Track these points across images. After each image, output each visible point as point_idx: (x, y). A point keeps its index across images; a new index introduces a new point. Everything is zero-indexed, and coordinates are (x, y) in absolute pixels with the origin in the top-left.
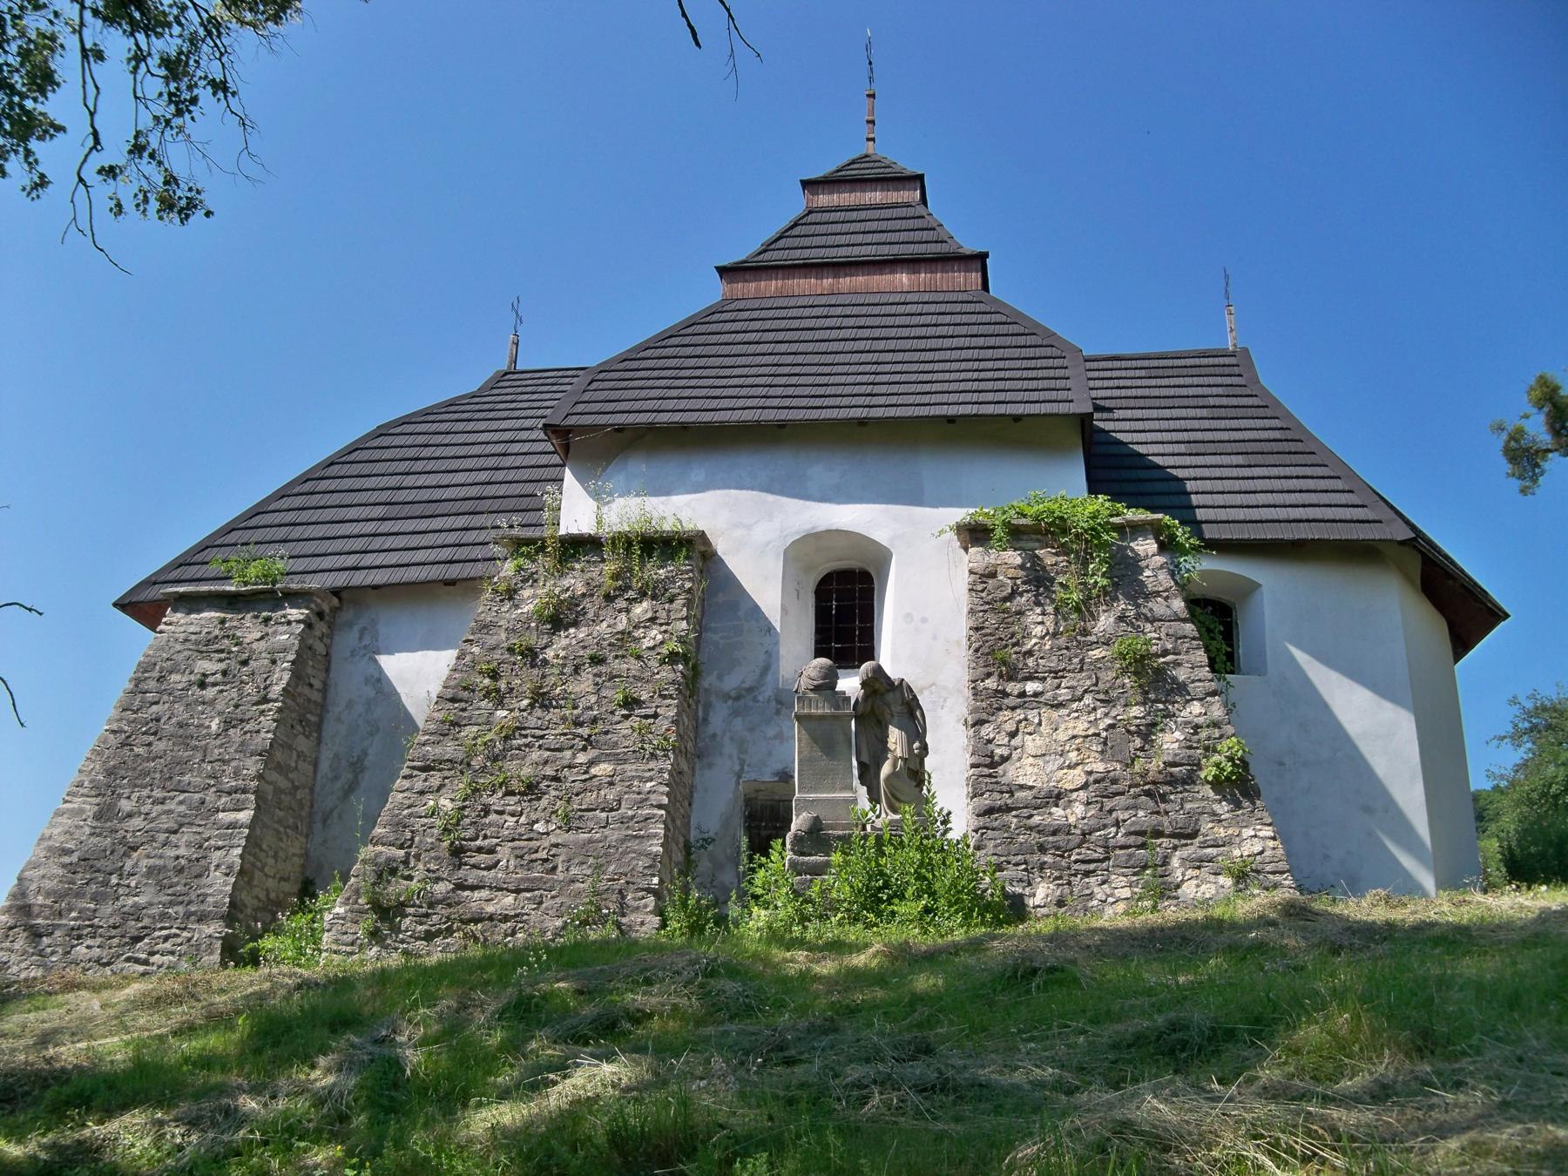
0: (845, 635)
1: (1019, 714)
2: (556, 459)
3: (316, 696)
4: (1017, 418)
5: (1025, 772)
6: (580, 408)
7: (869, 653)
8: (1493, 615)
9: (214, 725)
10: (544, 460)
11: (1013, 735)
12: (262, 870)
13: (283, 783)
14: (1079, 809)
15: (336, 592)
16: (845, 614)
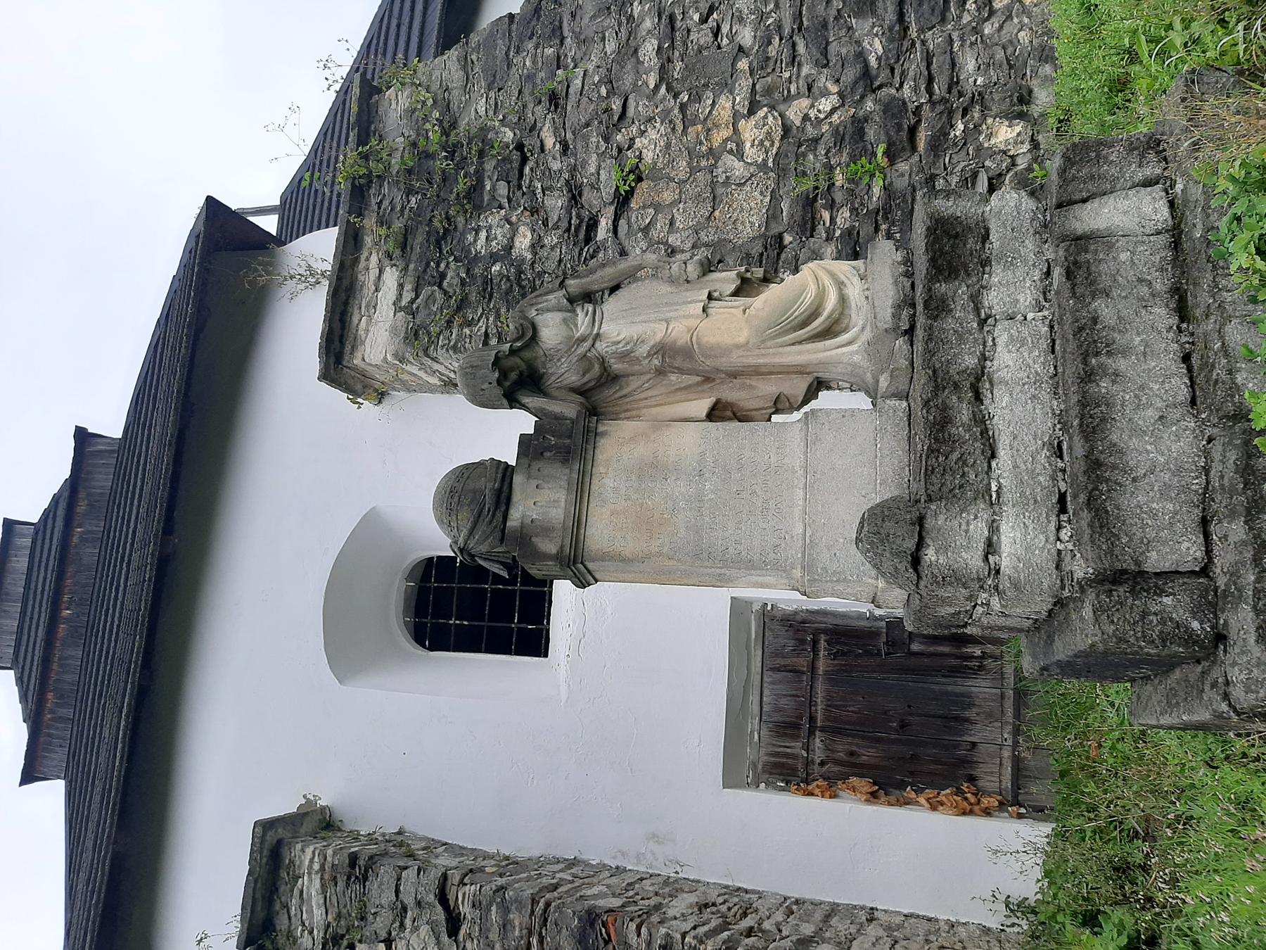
0: (503, 604)
11: (672, 252)
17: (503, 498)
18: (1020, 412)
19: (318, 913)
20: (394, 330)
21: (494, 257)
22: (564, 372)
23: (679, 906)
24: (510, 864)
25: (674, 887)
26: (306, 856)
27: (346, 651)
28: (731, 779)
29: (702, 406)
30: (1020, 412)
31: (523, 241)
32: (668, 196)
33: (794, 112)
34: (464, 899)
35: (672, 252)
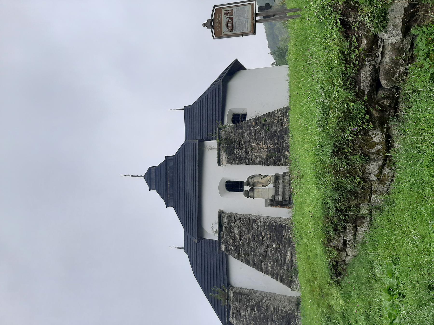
0: (238, 186)
1: (253, 157)
2: (203, 240)
3: (248, 291)
4: (199, 153)
5: (264, 155)
6: (194, 236)
7: (242, 182)
8: (236, 61)
9: (254, 313)
10: (203, 243)
11: (257, 158)
12: (283, 304)
13: (266, 298)
14: (272, 146)
15: (228, 286)
16: (234, 186)
17: (248, 194)
18: (281, 190)
19: (226, 221)
20: (226, 161)
21: (237, 154)
22: (251, 183)
23: (261, 218)
24: (244, 215)
25: (261, 217)
26: (224, 216)
27: (221, 194)
28: (266, 206)
29: (261, 186)
30: (281, 190)
31: (241, 153)
32: (256, 152)
33: (269, 145)
34: (242, 219)
35: (257, 158)
